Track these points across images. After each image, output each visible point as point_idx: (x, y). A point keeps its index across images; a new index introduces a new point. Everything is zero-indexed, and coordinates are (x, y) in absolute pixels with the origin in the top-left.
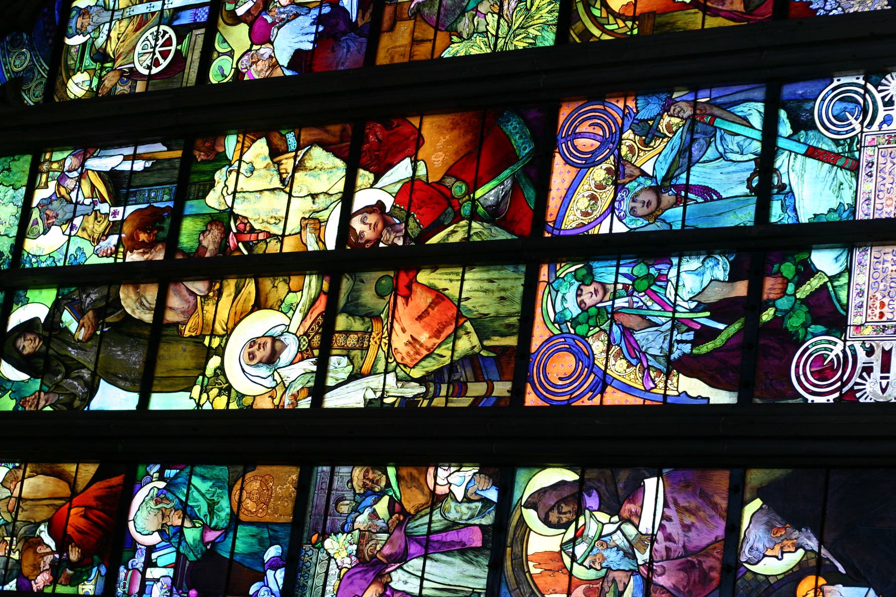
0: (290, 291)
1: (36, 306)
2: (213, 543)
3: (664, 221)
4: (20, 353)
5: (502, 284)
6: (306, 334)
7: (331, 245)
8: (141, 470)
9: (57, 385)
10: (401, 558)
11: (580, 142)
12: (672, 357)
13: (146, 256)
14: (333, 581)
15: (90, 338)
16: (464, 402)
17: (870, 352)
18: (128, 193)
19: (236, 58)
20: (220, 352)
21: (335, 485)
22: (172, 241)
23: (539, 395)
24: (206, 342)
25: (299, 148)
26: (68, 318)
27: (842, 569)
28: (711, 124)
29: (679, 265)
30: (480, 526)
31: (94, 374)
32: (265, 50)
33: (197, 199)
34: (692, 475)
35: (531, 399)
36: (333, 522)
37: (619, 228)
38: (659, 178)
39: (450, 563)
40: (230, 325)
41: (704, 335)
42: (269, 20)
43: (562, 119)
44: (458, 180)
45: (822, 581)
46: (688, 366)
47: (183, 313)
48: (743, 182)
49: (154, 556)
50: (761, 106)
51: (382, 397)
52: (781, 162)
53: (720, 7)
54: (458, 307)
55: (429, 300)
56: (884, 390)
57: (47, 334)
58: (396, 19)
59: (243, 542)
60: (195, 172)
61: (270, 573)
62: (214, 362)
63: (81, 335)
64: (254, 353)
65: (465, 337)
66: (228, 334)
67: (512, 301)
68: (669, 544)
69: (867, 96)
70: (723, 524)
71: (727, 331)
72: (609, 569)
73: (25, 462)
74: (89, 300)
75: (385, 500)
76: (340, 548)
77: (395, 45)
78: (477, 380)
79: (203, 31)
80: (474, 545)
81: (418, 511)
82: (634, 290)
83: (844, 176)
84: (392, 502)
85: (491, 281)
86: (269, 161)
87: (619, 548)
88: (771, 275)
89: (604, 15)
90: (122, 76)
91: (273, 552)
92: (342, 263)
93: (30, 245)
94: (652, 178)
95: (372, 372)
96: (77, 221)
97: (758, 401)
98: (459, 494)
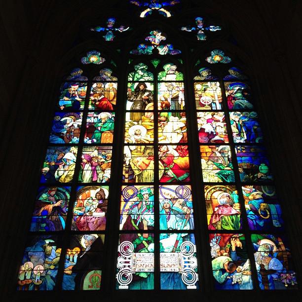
5: (149, 178)
7: (159, 143)
10: (92, 166)
11: (181, 190)
12: (131, 215)
14: (88, 153)
16: (124, 173)
17: (129, 259)
20: (138, 124)
22: (163, 111)
26: (147, 94)
34: (105, 223)
35: (124, 187)
37: (160, 201)
41: (136, 221)
43: (187, 186)
45: (79, 253)
46: (129, 218)
49: (96, 118)
50: (189, 229)
52: (175, 235)
58: (212, 148)
59: (97, 135)
62: (136, 123)
63: (143, 97)
64: (137, 131)
66: (142, 125)
70: (93, 230)
71: (136, 227)
75: (104, 161)
76: (95, 153)
77: (205, 149)
78: (129, 175)
83: (171, 249)
84: (103, 162)
91: (95, 141)
92: (156, 145)
93: (163, 84)
95: (132, 154)
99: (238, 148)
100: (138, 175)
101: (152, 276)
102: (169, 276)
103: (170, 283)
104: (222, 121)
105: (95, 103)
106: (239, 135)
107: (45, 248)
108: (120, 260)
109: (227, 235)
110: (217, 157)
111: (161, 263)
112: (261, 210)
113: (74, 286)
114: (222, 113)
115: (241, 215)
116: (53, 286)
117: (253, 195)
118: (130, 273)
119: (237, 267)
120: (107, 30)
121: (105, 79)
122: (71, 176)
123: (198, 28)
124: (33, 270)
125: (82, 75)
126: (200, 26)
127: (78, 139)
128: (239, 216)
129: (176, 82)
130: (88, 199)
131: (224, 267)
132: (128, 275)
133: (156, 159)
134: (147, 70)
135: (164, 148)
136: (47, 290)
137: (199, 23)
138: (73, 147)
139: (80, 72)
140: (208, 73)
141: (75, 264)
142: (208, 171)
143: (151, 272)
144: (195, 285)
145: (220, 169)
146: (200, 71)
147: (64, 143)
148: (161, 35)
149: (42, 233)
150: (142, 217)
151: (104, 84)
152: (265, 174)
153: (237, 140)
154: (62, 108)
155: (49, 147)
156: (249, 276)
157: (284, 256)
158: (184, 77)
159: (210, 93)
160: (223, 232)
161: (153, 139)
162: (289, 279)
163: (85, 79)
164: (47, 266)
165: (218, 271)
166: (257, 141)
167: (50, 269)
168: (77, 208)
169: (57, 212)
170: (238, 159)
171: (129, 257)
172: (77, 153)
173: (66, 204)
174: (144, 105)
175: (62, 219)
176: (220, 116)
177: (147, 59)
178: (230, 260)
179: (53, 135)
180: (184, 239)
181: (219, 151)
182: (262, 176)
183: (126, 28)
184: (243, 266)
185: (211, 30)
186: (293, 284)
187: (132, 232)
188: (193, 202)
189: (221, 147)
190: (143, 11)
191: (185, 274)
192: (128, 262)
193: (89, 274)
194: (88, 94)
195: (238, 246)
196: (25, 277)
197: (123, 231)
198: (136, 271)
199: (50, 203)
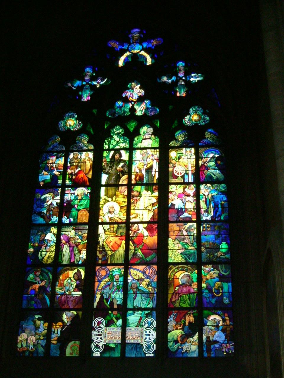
0: (123, 213)
1: (125, 156)
2: (75, 207)
4: (115, 155)
5: (121, 258)
6: (114, 219)
7: (131, 221)
8: (90, 188)
9: (108, 165)
10: (70, 246)
11: (148, 270)
13: (133, 179)
15: (118, 171)
17: (101, 332)
19: (175, 191)
20: (112, 200)
21: (84, 230)
22: (136, 184)
23: (99, 269)
24: (114, 197)
25: (153, 209)
26: (122, 164)
28: (149, 297)
29: (121, 294)
30: (75, 261)
31: (110, 173)
32: (176, 197)
33: (145, 188)
35: (98, 268)
36: (77, 231)
37: (129, 281)
38: (139, 288)
39: (68, 256)
40: (117, 202)
41: (107, 300)
42: (183, 197)
44: (143, 246)
45: (61, 326)
46: (102, 298)
47: (121, 190)
48: (136, 305)
49: (73, 195)
50: (151, 307)
51: (100, 237)
52: (140, 312)
53: (174, 296)
54: (117, 250)
55: (119, 244)
56: (94, 335)
57: (119, 160)
59: (74, 213)
60: (151, 187)
61: (68, 220)
62: (110, 199)
63: (118, 168)
64: (111, 208)
65: (111, 252)
66: (116, 201)
67: (117, 261)
68: (69, 298)
69: (151, 328)
70: (72, 307)
72: (65, 287)
73: (94, 162)
74: (125, 168)
77: (173, 227)
78: (102, 256)
79: (182, 181)
80: (71, 260)
81: (78, 248)
82: (117, 285)
83: (136, 324)
84: (80, 243)
85: (121, 256)
86: (151, 203)
87: (69, 288)
88: (118, 312)
89: (175, 272)
90: (175, 164)
91: (72, 220)
92: (128, 224)
93: (138, 151)
94: (139, 286)
95: (105, 234)
96: (143, 161)
97: (94, 312)
99: (204, 225)
100: (110, 256)
101: (119, 347)
102: (132, 346)
103: (133, 352)
104: (192, 195)
106: (207, 211)
107: (35, 322)
108: (95, 333)
109: (183, 311)
110: (184, 236)
112: (215, 288)
113: (59, 353)
115: (198, 293)
116: (43, 352)
117: (210, 274)
118: (102, 344)
119: (188, 339)
120: (84, 83)
121: (81, 148)
122: (52, 256)
123: (179, 77)
124: (27, 340)
125: (60, 143)
126: (181, 75)
127: (57, 219)
128: (195, 294)
130: (67, 279)
131: (177, 338)
132: (100, 345)
133: (128, 239)
134: (123, 135)
135: (135, 227)
136: (39, 355)
137: (180, 70)
138: (53, 227)
139: (58, 139)
140: (185, 137)
141: (59, 335)
142: (174, 251)
143: (118, 343)
147: (45, 222)
148: (140, 88)
149: (32, 310)
150: (113, 296)
151: (80, 153)
153: (205, 217)
154: (42, 184)
156: (196, 346)
157: (227, 329)
158: (160, 143)
159: (184, 161)
160: (181, 309)
161: (125, 218)
162: (228, 348)
163: (62, 148)
164: (38, 337)
166: (222, 218)
167: (40, 339)
168: (58, 288)
170: (203, 237)
171: (101, 330)
172: (56, 233)
174: (118, 178)
176: (191, 190)
177: (122, 121)
178: (183, 333)
179: (35, 215)
180: (147, 315)
181: (186, 229)
182: (221, 255)
183: (103, 81)
184: (192, 338)
185: (192, 79)
186: (230, 352)
187: (104, 310)
188: (157, 281)
189: (189, 225)
190: (122, 55)
191: (145, 345)
192: (101, 335)
193: (71, 344)
194: (66, 167)
195: (191, 321)
196: (22, 345)
198: (107, 342)
199: (36, 283)
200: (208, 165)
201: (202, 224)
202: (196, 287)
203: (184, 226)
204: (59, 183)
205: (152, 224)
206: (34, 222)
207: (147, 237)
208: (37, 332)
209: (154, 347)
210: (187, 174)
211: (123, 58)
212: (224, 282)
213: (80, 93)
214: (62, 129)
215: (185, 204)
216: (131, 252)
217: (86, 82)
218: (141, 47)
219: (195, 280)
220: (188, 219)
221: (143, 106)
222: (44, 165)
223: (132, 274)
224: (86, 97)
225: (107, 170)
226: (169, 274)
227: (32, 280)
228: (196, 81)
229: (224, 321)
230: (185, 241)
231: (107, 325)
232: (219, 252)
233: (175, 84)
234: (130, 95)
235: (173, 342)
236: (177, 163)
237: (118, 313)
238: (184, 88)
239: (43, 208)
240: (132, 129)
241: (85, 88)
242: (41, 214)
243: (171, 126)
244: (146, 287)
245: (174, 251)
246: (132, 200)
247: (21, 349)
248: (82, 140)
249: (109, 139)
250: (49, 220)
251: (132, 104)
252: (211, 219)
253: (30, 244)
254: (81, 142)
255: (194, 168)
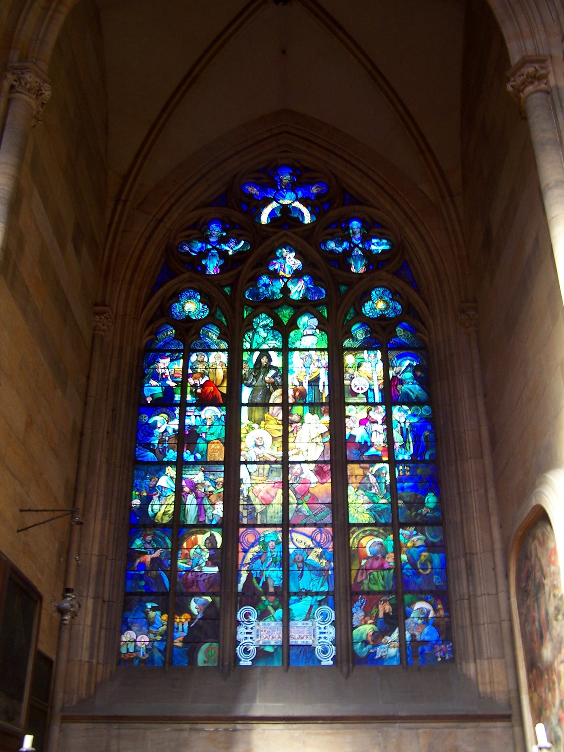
1: (277, 360)
2: (201, 437)
3: (293, 564)
7: (290, 459)
8: (224, 408)
10: (197, 497)
11: (319, 535)
17: (252, 628)
18: (311, 386)
19: (356, 415)
20: (260, 428)
22: (295, 404)
24: (263, 422)
26: (272, 372)
27: (192, 625)
31: (254, 386)
35: (241, 530)
37: (291, 551)
45: (189, 620)
46: (249, 577)
49: (198, 417)
50: (326, 591)
52: (309, 598)
59: (202, 446)
61: (193, 456)
62: (256, 426)
63: (267, 379)
64: (259, 438)
73: (228, 368)
77: (354, 470)
79: (366, 401)
83: (304, 617)
84: (212, 492)
85: (277, 513)
90: (353, 375)
91: (199, 456)
92: (285, 463)
93: (297, 353)
96: (304, 369)
97: (239, 598)
98: (214, 512)
101: (280, 650)
104: (380, 422)
105: (196, 391)
106: (403, 446)
107: (147, 613)
108: (241, 630)
111: (290, 634)
113: (186, 661)
114: (382, 409)
115: (395, 569)
116: (162, 661)
119: (383, 637)
120: (209, 247)
121: (209, 346)
127: (175, 454)
128: (392, 571)
129: (316, 350)
130: (195, 547)
133: (285, 485)
134: (272, 328)
135: (296, 469)
137: (354, 233)
139: (172, 332)
140: (366, 334)
141: (185, 634)
143: (278, 646)
144: (332, 659)
145: (374, 503)
146: (353, 329)
148: (294, 257)
151: (207, 354)
152: (432, 509)
154: (149, 400)
155: (136, 467)
159: (366, 371)
160: (369, 593)
161: (280, 454)
165: (360, 644)
166: (427, 457)
168: (181, 561)
169: (157, 565)
170: (399, 485)
171: (251, 626)
172: (175, 477)
173: (167, 555)
174: (268, 393)
175: (164, 575)
176: (378, 414)
177: (270, 306)
180: (320, 603)
181: (373, 473)
182: (428, 512)
184: (390, 636)
185: (373, 247)
189: (378, 466)
190: (266, 206)
192: (250, 633)
194: (186, 376)
195: (387, 611)
196: (128, 649)
197: (243, 593)
198: (261, 643)
199: (146, 553)
200: (403, 378)
201: (398, 465)
202: (393, 561)
203: (371, 469)
204: (175, 399)
205: (323, 465)
206: (140, 459)
207: (316, 485)
208: (151, 629)
209: (332, 650)
210: (373, 390)
211: (266, 211)
212: (433, 553)
213: (204, 262)
214: (178, 316)
215: (370, 435)
216: (292, 507)
217: (210, 245)
218: (293, 195)
219: (390, 549)
220: (374, 459)
221: (301, 284)
222: (152, 370)
223: (294, 540)
224: (212, 266)
225: (249, 382)
226: (351, 540)
227: (139, 548)
228: (380, 251)
229: (436, 610)
230: (373, 491)
231: (260, 618)
232: (425, 509)
233: (348, 253)
234: (281, 267)
235: (362, 644)
236: (357, 372)
237: (275, 600)
238: (361, 261)
239: (153, 438)
240: (285, 321)
241: (210, 254)
242: (149, 446)
243: (345, 316)
244: (317, 560)
245: (357, 505)
246: (290, 427)
247: (127, 655)
248: (210, 334)
249: (251, 334)
250: (162, 456)
251: (283, 281)
252: (410, 458)
253: (134, 492)
254: (208, 337)
255: (383, 381)
